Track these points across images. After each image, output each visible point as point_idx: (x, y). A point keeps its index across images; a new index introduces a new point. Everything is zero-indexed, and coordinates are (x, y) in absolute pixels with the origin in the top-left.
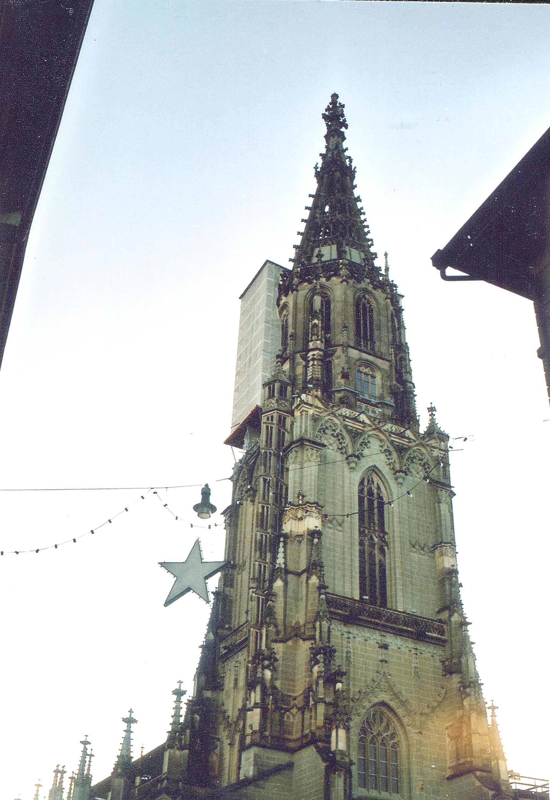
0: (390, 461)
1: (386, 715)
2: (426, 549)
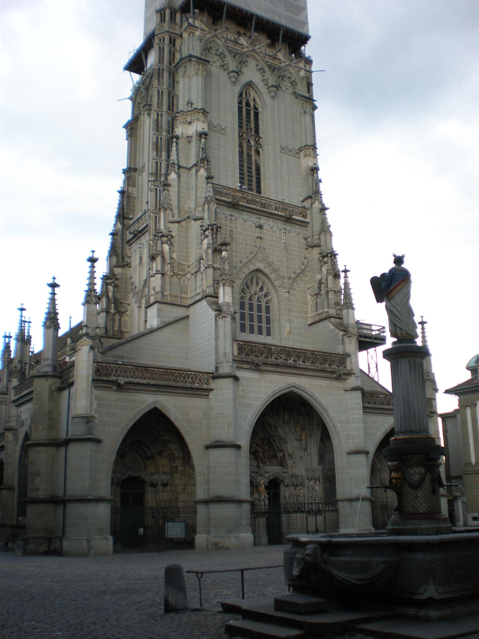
0: (265, 78)
1: (261, 279)
2: (293, 151)
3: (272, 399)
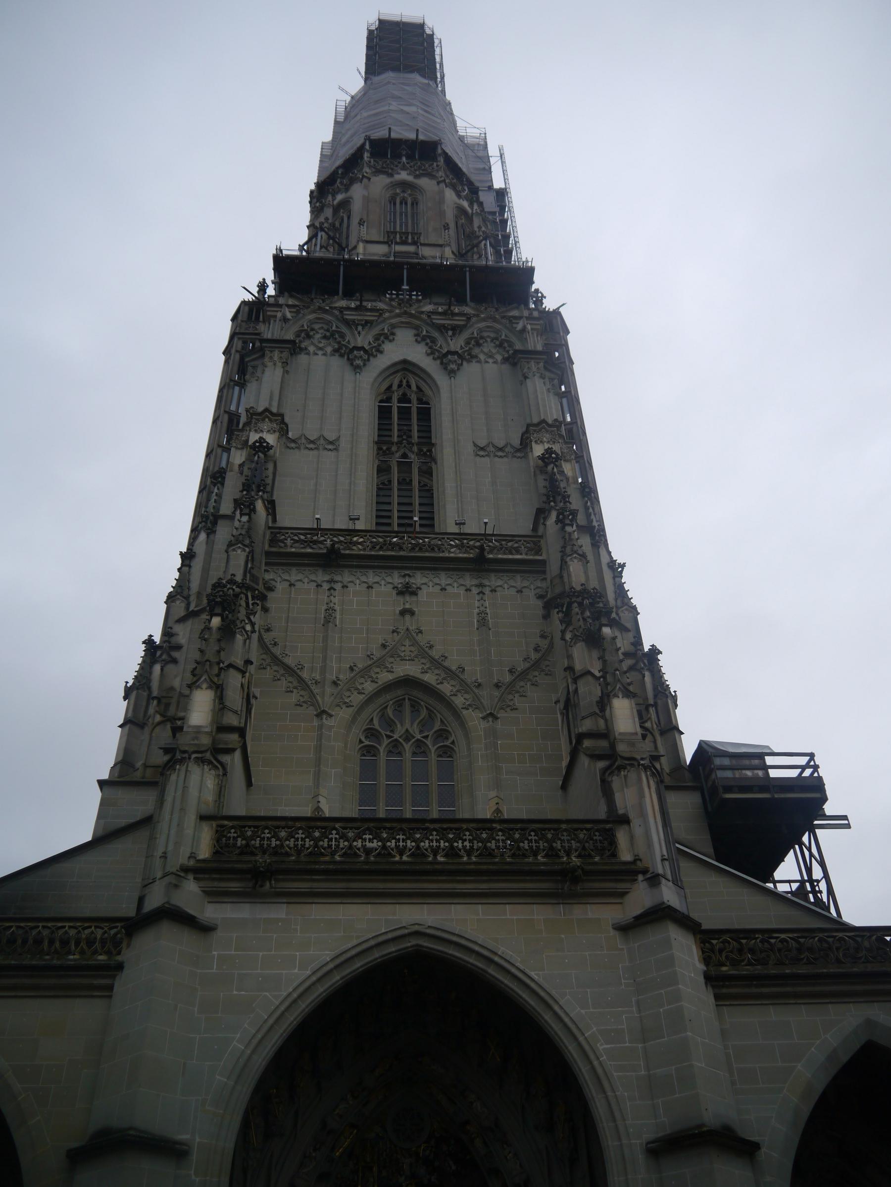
1: (422, 703)
2: (508, 449)
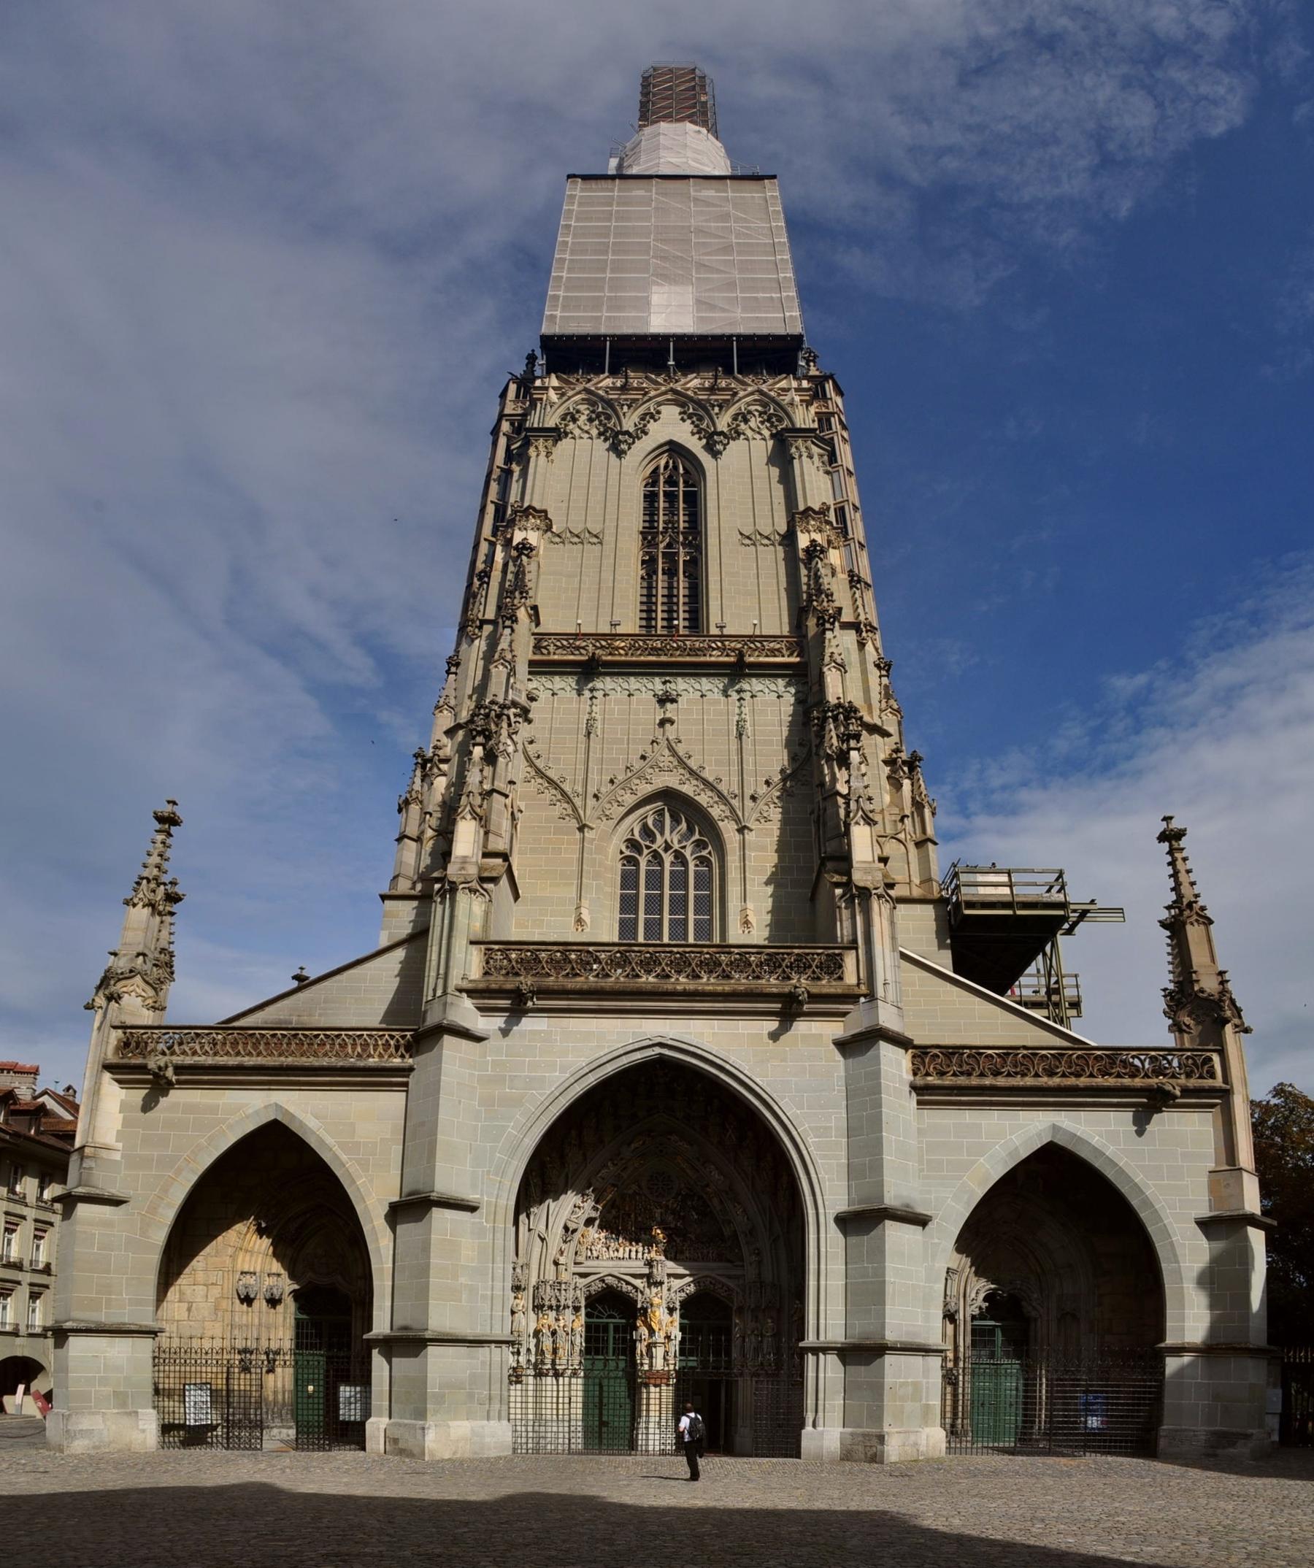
3: (592, 1080)
